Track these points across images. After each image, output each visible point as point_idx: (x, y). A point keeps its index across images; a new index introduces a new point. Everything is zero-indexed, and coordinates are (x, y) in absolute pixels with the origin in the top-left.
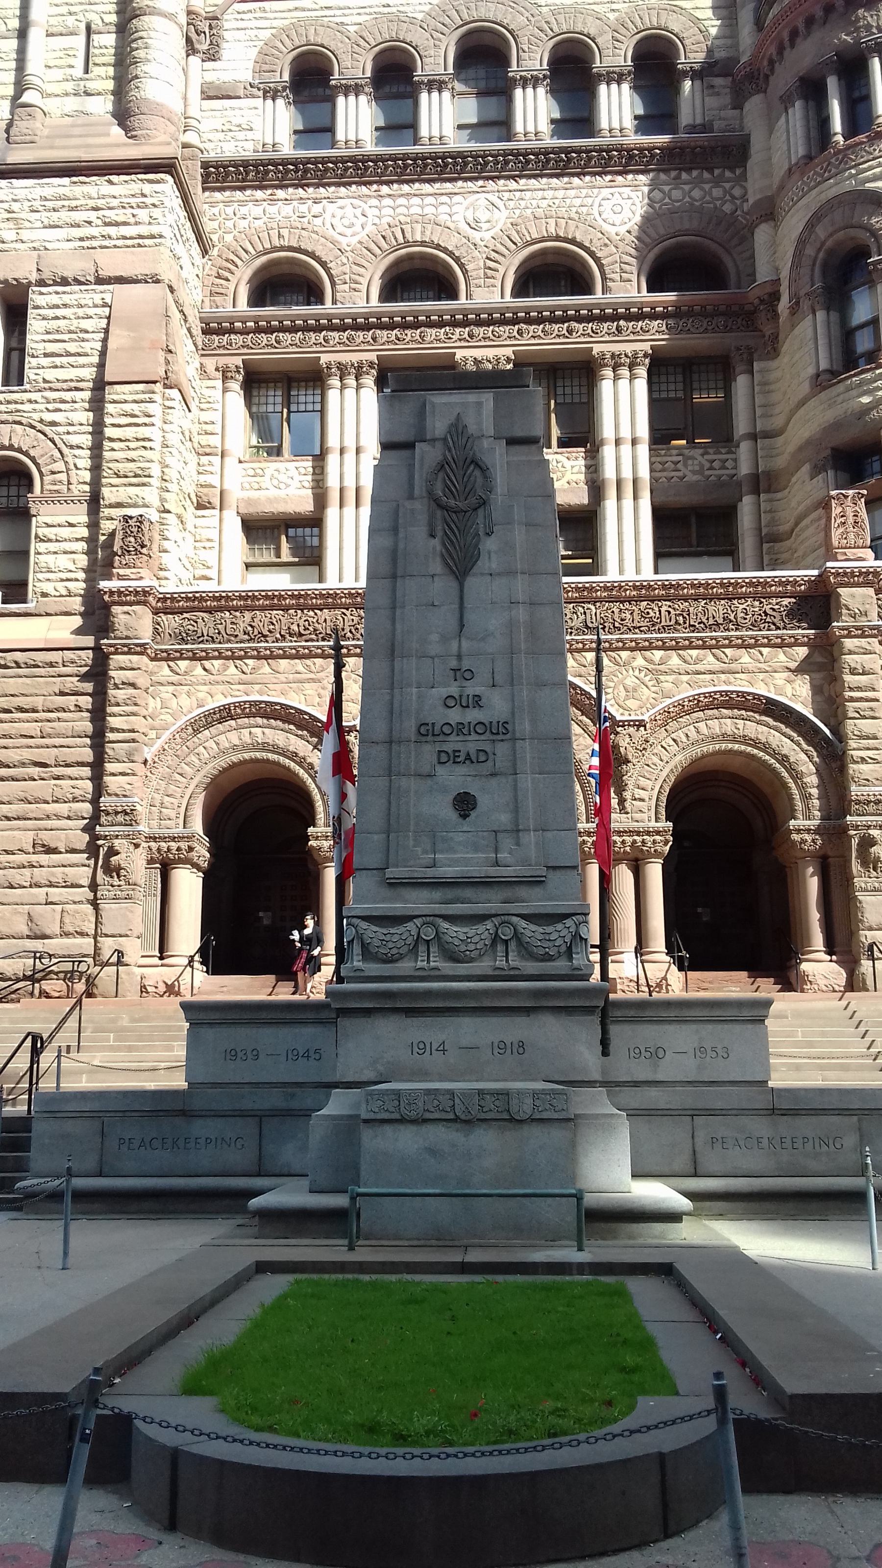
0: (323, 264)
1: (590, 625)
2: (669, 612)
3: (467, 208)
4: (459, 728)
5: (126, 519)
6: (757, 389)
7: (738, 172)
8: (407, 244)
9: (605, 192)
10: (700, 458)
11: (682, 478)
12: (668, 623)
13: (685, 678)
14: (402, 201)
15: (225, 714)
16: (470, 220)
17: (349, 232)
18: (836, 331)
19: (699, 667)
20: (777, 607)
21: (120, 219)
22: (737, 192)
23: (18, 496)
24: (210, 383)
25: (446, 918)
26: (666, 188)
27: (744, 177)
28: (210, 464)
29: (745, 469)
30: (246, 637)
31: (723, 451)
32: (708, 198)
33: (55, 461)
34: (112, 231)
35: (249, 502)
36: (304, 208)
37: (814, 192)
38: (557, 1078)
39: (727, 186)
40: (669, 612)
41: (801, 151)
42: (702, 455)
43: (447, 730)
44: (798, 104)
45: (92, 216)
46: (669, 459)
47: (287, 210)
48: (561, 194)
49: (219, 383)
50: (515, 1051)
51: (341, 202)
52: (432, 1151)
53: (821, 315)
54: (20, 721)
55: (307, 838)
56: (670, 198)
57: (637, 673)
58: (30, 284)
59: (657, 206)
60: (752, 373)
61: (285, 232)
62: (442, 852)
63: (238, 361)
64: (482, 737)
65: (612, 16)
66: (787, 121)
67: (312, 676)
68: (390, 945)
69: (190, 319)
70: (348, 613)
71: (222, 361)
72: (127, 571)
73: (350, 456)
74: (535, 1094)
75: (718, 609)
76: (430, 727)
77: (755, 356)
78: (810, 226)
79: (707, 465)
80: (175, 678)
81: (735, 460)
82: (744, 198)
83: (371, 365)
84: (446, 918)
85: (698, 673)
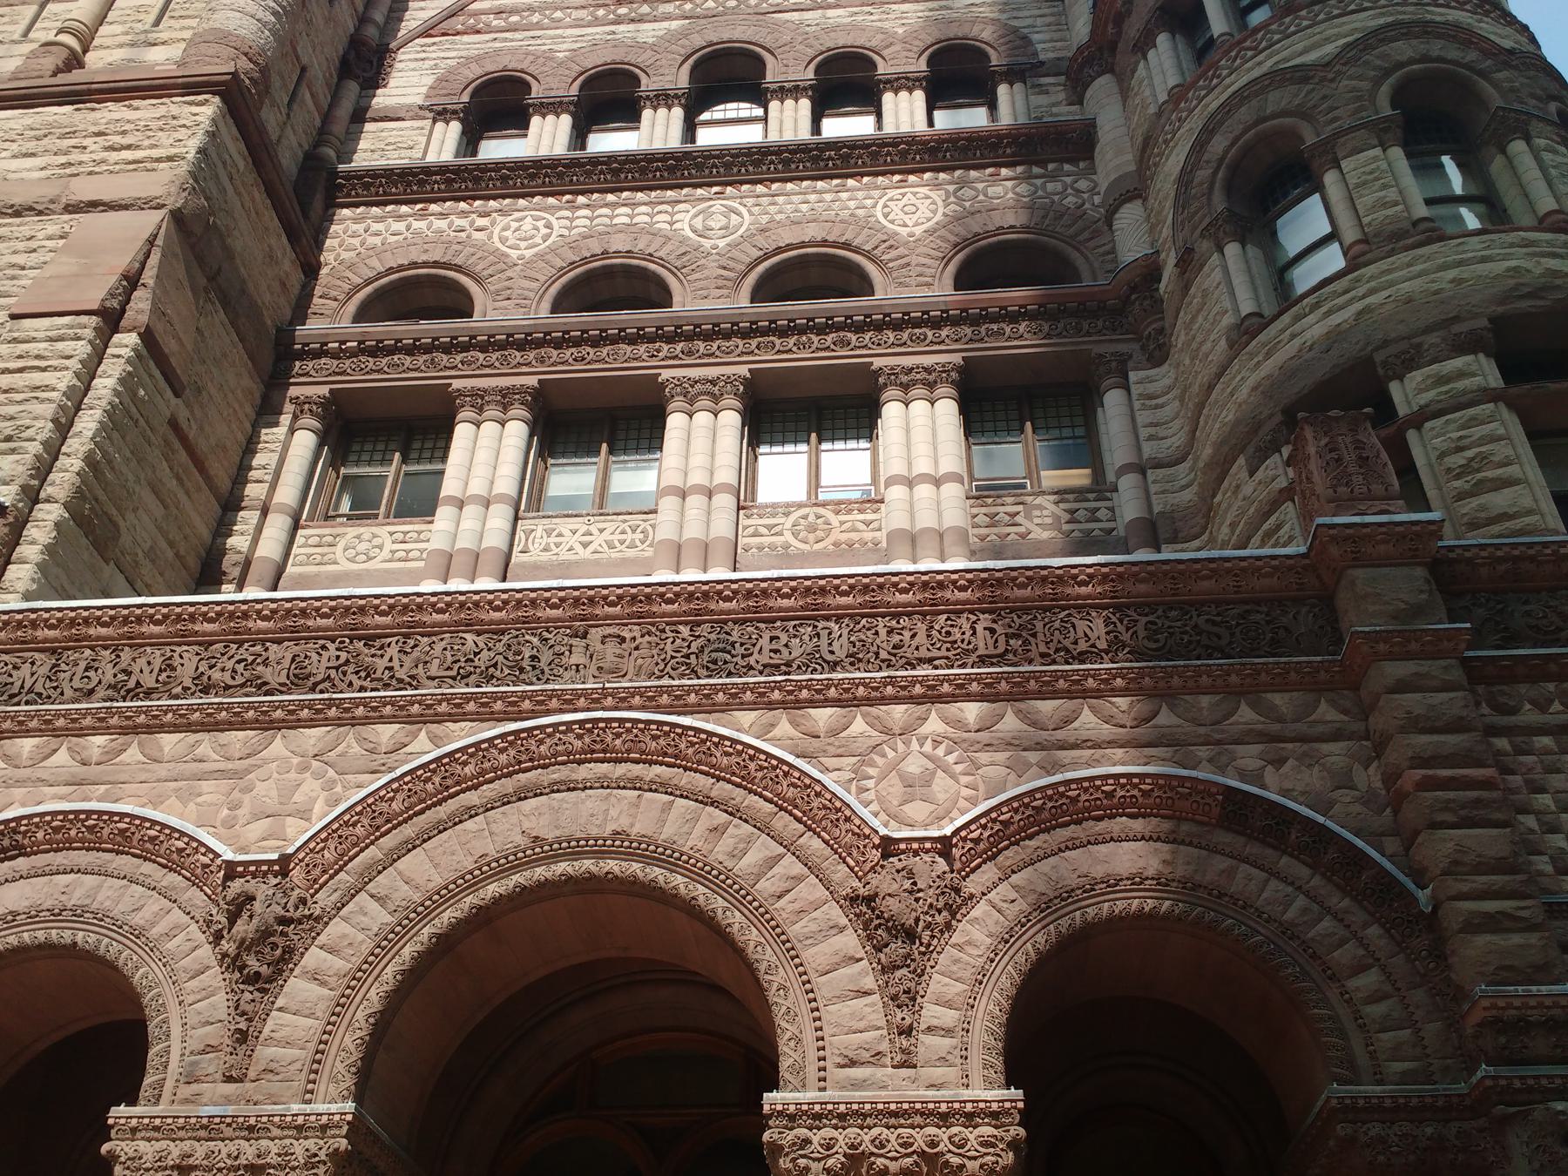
1: (829, 657)
2: (992, 631)
3: (696, 216)
6: (1137, 405)
9: (892, 193)
10: (1052, 507)
11: (1023, 536)
12: (991, 651)
13: (1033, 757)
16: (700, 227)
18: (1258, 266)
19: (1060, 735)
20: (1219, 619)
26: (980, 186)
27: (1092, 170)
32: (1040, 193)
39: (1068, 180)
42: (1056, 503)
44: (1163, 39)
46: (1001, 509)
47: (442, 224)
51: (517, 215)
53: (1232, 249)
56: (986, 195)
57: (928, 747)
65: (900, 31)
66: (1148, 68)
77: (1130, 364)
78: (1200, 146)
81: (1112, 509)
82: (1093, 191)
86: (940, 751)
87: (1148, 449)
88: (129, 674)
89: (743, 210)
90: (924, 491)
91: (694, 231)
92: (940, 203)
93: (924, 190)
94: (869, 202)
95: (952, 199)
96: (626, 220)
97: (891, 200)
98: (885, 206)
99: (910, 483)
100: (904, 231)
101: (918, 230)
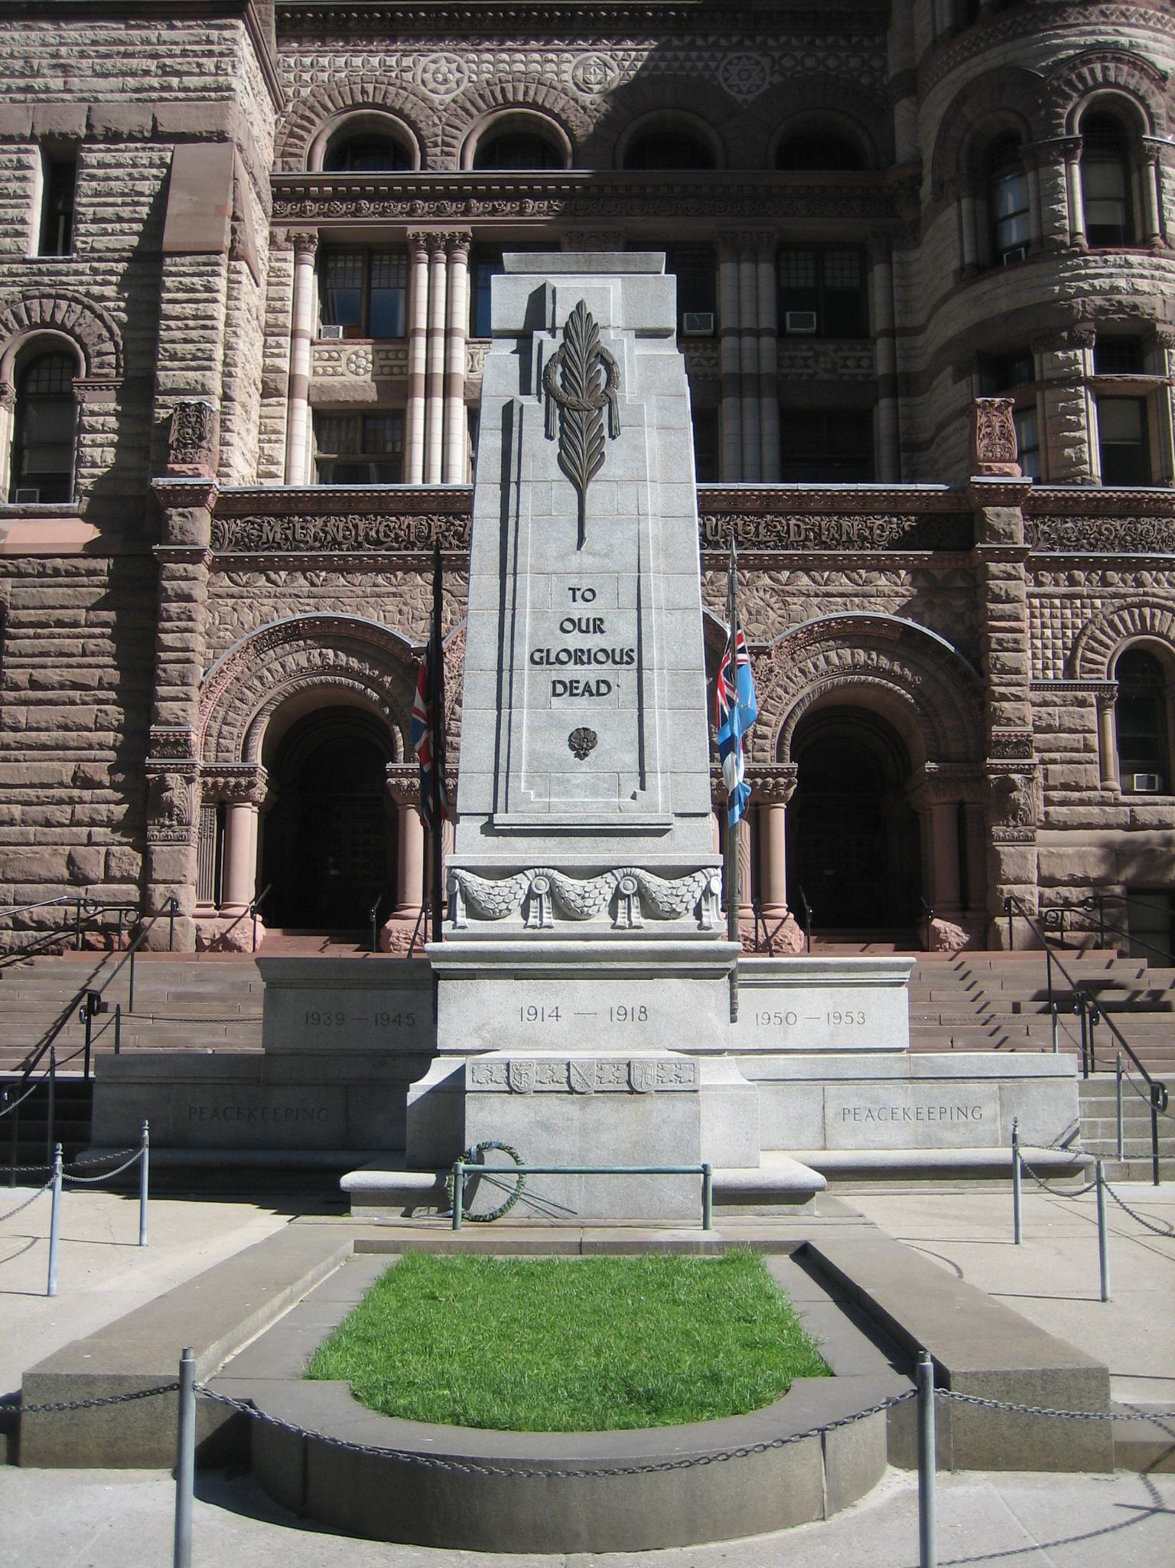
0: (413, 124)
2: (798, 526)
4: (578, 657)
5: (184, 406)
6: (896, 282)
7: (878, 40)
8: (507, 104)
9: (732, 56)
13: (815, 601)
14: (505, 56)
15: (291, 633)
17: (442, 88)
21: (185, 68)
22: (876, 63)
23: (61, 380)
24: (281, 255)
25: (561, 870)
28: (279, 346)
29: (882, 368)
30: (317, 544)
31: (858, 348)
33: (104, 341)
34: (175, 81)
35: (321, 389)
36: (392, 61)
37: (963, 67)
38: (681, 1047)
39: (866, 55)
40: (798, 526)
41: (947, 21)
43: (564, 657)
45: (152, 65)
48: (681, 55)
49: (290, 256)
50: (636, 1017)
51: (434, 56)
52: (545, 1126)
53: (965, 203)
54: (60, 636)
55: (387, 775)
58: (79, 140)
59: (788, 74)
60: (889, 262)
61: (370, 88)
62: (557, 795)
63: (314, 231)
64: (604, 666)
67: (394, 590)
68: (499, 899)
69: (260, 182)
70: (435, 518)
71: (295, 230)
72: (184, 467)
73: (439, 341)
74: (661, 1065)
75: (852, 525)
76: (544, 654)
79: (841, 362)
80: (236, 590)
81: (871, 359)
82: (884, 69)
83: (464, 237)
84: (561, 870)
85: (828, 595)
86: (768, 596)
87: (897, 323)
88: (326, 533)
89: (614, 64)
90: (748, 342)
91: (576, 84)
92: (768, 71)
93: (754, 55)
94: (713, 64)
95: (777, 68)
96: (522, 67)
97: (730, 63)
98: (726, 70)
99: (739, 333)
100: (740, 97)
101: (750, 97)
